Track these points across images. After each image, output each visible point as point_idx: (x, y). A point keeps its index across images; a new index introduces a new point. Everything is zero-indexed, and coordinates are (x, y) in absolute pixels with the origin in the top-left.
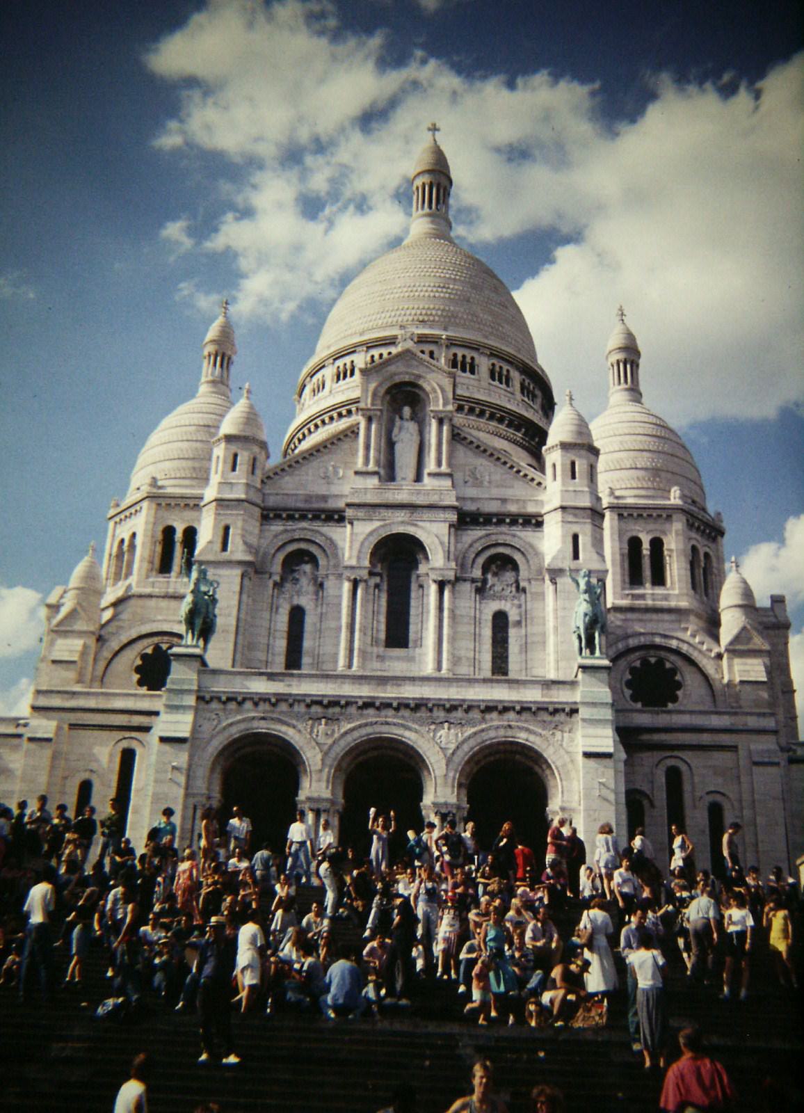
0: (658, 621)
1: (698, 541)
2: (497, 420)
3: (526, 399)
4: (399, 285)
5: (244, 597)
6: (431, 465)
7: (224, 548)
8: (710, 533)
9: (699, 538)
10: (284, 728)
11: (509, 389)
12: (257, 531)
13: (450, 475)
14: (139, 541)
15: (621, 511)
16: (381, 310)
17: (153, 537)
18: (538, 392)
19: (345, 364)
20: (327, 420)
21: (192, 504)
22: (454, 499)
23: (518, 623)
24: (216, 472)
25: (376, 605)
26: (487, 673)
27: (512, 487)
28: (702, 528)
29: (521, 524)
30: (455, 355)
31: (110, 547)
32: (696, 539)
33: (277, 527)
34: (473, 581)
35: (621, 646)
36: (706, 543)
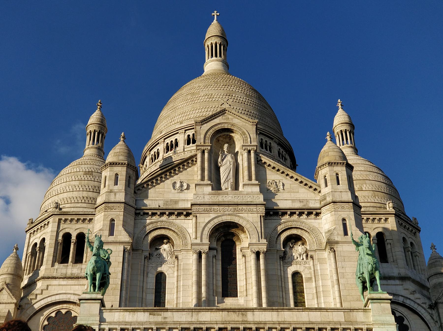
0: (387, 285)
3: (281, 160)
4: (202, 95)
7: (111, 233)
8: (412, 230)
9: (406, 233)
11: (272, 154)
12: (132, 223)
14: (47, 243)
16: (192, 109)
18: (288, 157)
19: (172, 141)
22: (263, 200)
23: (309, 279)
24: (105, 187)
25: (214, 269)
27: (298, 192)
29: (306, 215)
32: (404, 233)
36: (409, 235)
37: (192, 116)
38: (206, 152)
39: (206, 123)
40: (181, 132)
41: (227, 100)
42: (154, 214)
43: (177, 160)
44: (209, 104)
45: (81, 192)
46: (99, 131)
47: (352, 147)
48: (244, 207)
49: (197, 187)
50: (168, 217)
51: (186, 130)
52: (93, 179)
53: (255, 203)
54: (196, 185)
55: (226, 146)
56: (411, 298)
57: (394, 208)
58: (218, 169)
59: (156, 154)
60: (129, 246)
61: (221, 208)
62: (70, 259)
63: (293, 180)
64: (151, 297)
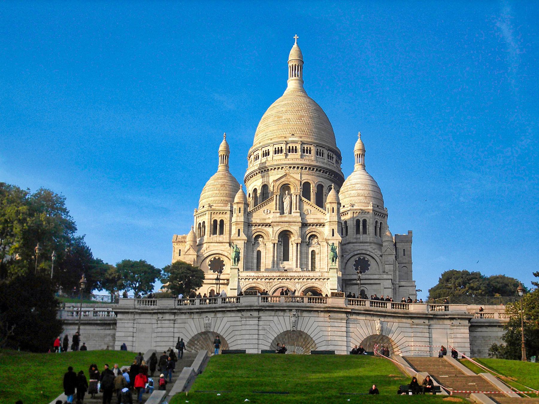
3: (329, 160)
5: (245, 249)
6: (293, 210)
7: (239, 235)
8: (383, 216)
9: (379, 218)
10: (259, 285)
11: (323, 158)
14: (206, 224)
15: (354, 211)
17: (211, 223)
18: (334, 156)
19: (266, 150)
21: (222, 212)
26: (310, 268)
27: (317, 214)
29: (319, 226)
30: (304, 147)
31: (196, 226)
34: (306, 242)
35: (352, 254)
36: (381, 219)
38: (278, 196)
42: (256, 225)
47: (361, 165)
48: (293, 223)
55: (287, 192)
56: (373, 252)
57: (373, 206)
58: (283, 203)
59: (257, 156)
62: (218, 233)
63: (315, 208)
64: (255, 265)
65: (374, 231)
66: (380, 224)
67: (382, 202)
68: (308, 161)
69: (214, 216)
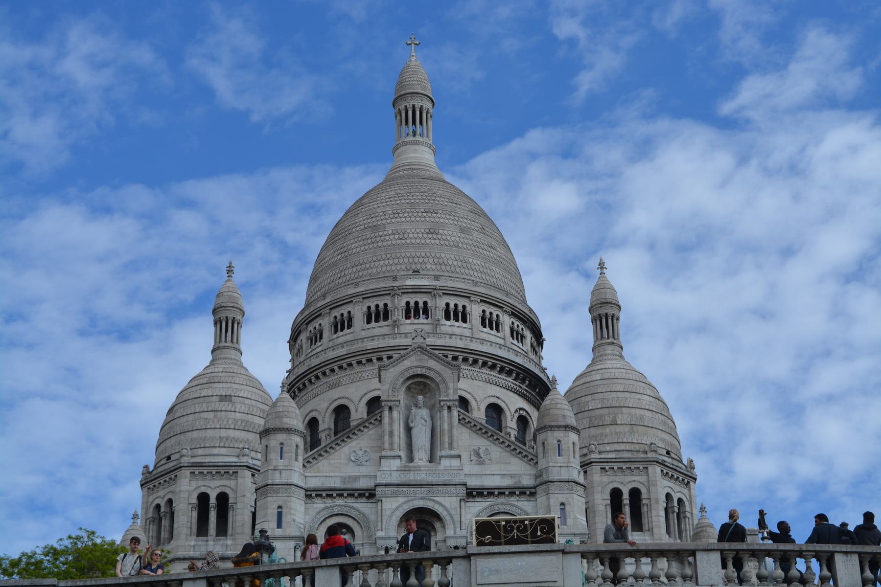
1: (672, 488)
2: (489, 368)
3: (515, 342)
4: (390, 232)
7: (279, 525)
8: (683, 480)
9: (672, 485)
12: (303, 509)
13: (459, 456)
16: (375, 259)
18: (528, 334)
19: (342, 315)
20: (328, 372)
21: (222, 472)
24: (266, 460)
27: (509, 463)
28: (675, 477)
29: (518, 496)
30: (447, 305)
32: (669, 487)
33: (319, 505)
36: (677, 487)
37: (374, 270)
39: (394, 366)
40: (357, 300)
41: (421, 331)
43: (351, 352)
44: (400, 251)
45: (217, 430)
46: (234, 318)
47: (613, 343)
48: (440, 488)
49: (383, 461)
50: (346, 499)
51: (364, 298)
52: (233, 409)
53: (454, 482)
54: (381, 458)
59: (317, 332)
60: (301, 541)
61: (412, 489)
65: (663, 520)
66: (679, 505)
67: (677, 444)
68: (461, 339)
69: (200, 483)
